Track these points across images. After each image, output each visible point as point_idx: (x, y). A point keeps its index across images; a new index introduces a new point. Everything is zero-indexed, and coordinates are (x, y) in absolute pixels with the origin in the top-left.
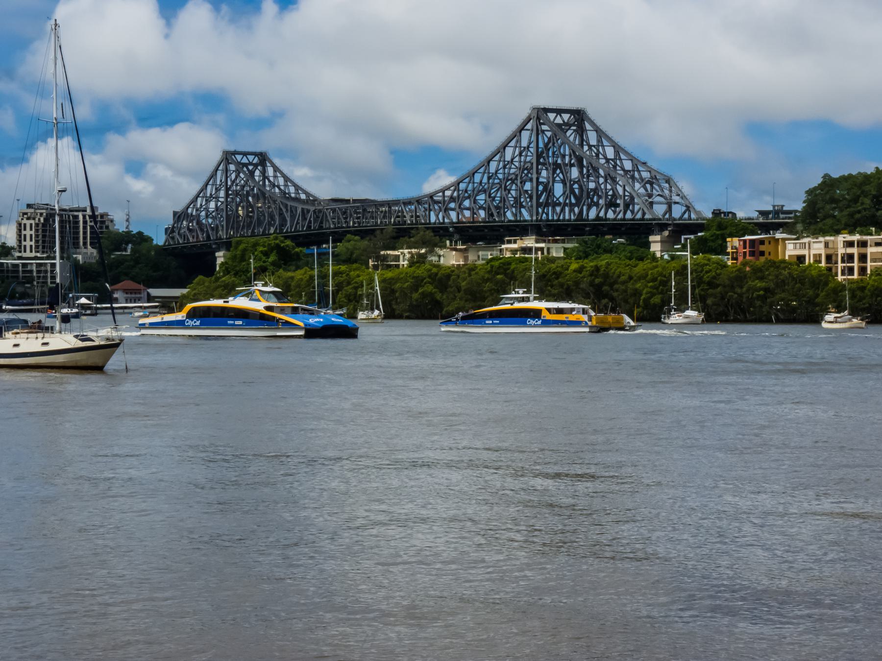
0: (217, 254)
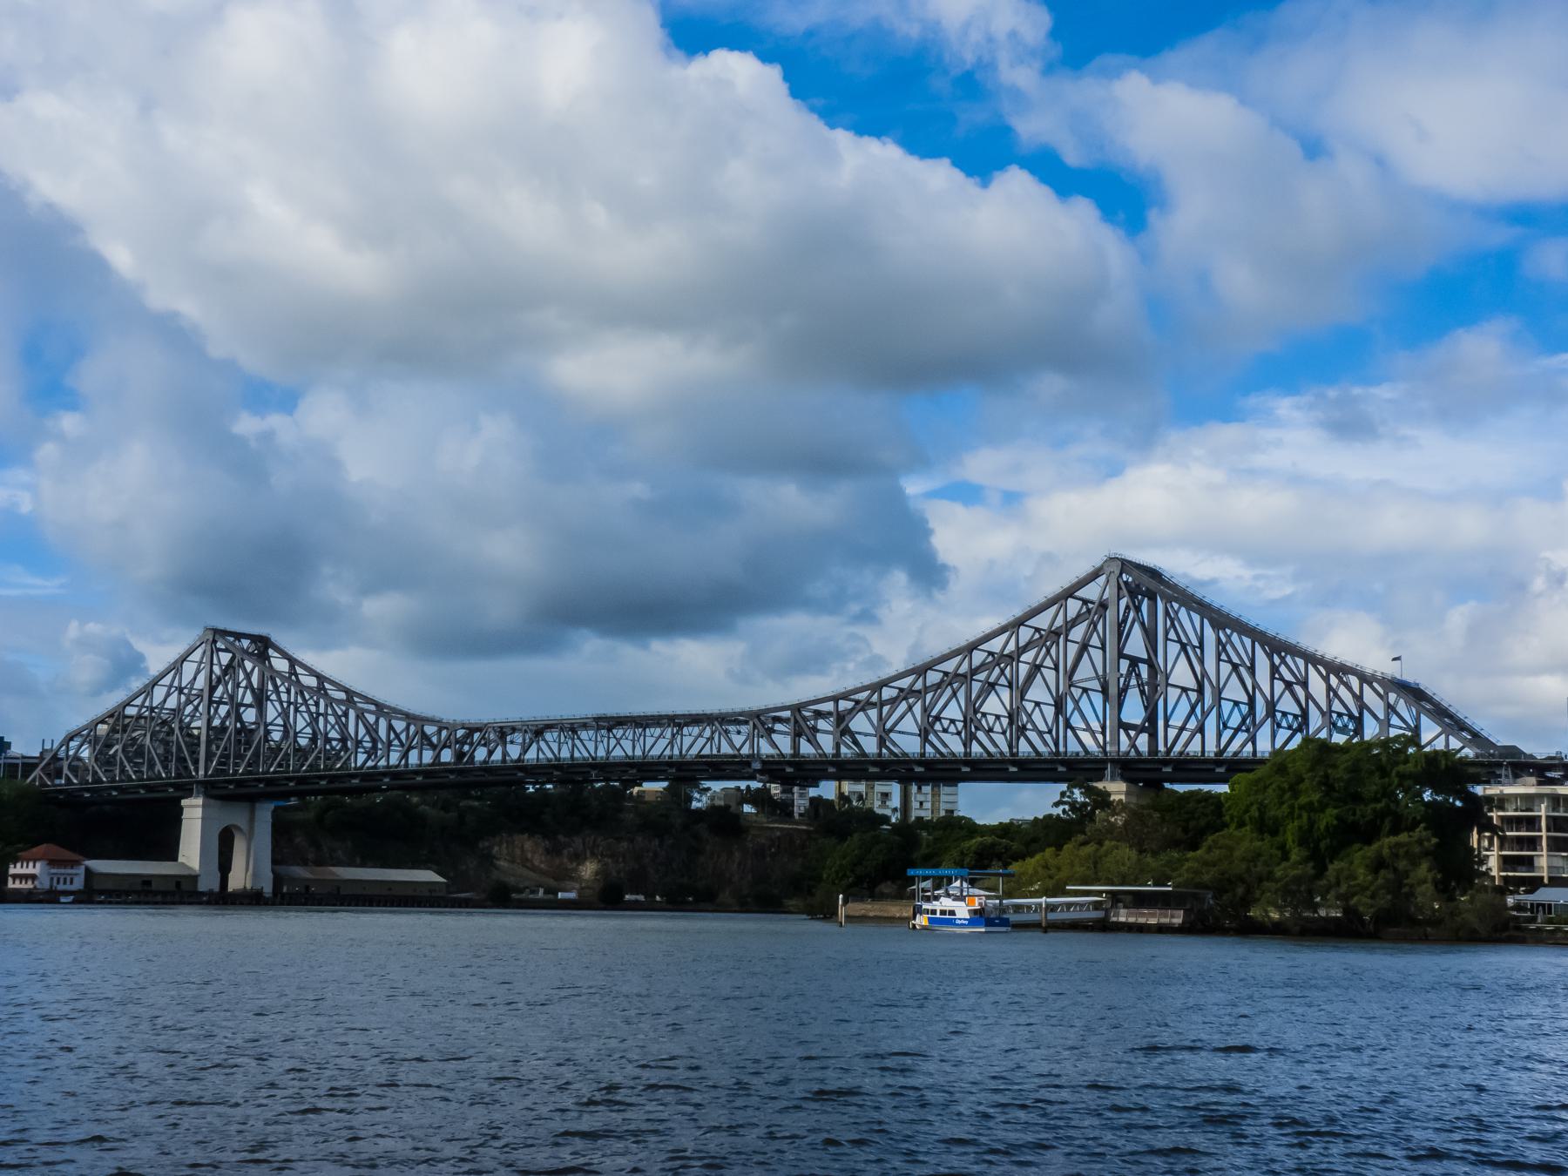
0: (184, 802)
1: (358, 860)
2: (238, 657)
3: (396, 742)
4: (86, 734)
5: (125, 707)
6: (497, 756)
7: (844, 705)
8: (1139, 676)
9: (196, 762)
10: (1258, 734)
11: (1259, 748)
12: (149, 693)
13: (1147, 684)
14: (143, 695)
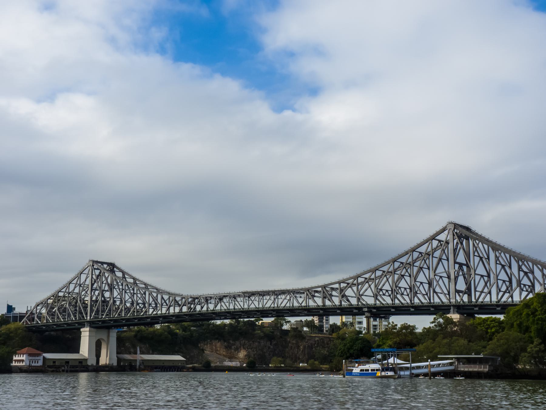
0: (82, 330)
1: (151, 352)
2: (102, 271)
3: (165, 304)
4: (44, 303)
5: (58, 293)
6: (205, 309)
7: (343, 285)
8: (463, 270)
9: (86, 314)
10: (514, 294)
11: (514, 300)
12: (68, 287)
13: (467, 274)
14: (66, 288)
